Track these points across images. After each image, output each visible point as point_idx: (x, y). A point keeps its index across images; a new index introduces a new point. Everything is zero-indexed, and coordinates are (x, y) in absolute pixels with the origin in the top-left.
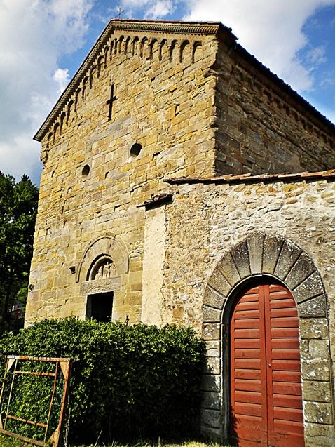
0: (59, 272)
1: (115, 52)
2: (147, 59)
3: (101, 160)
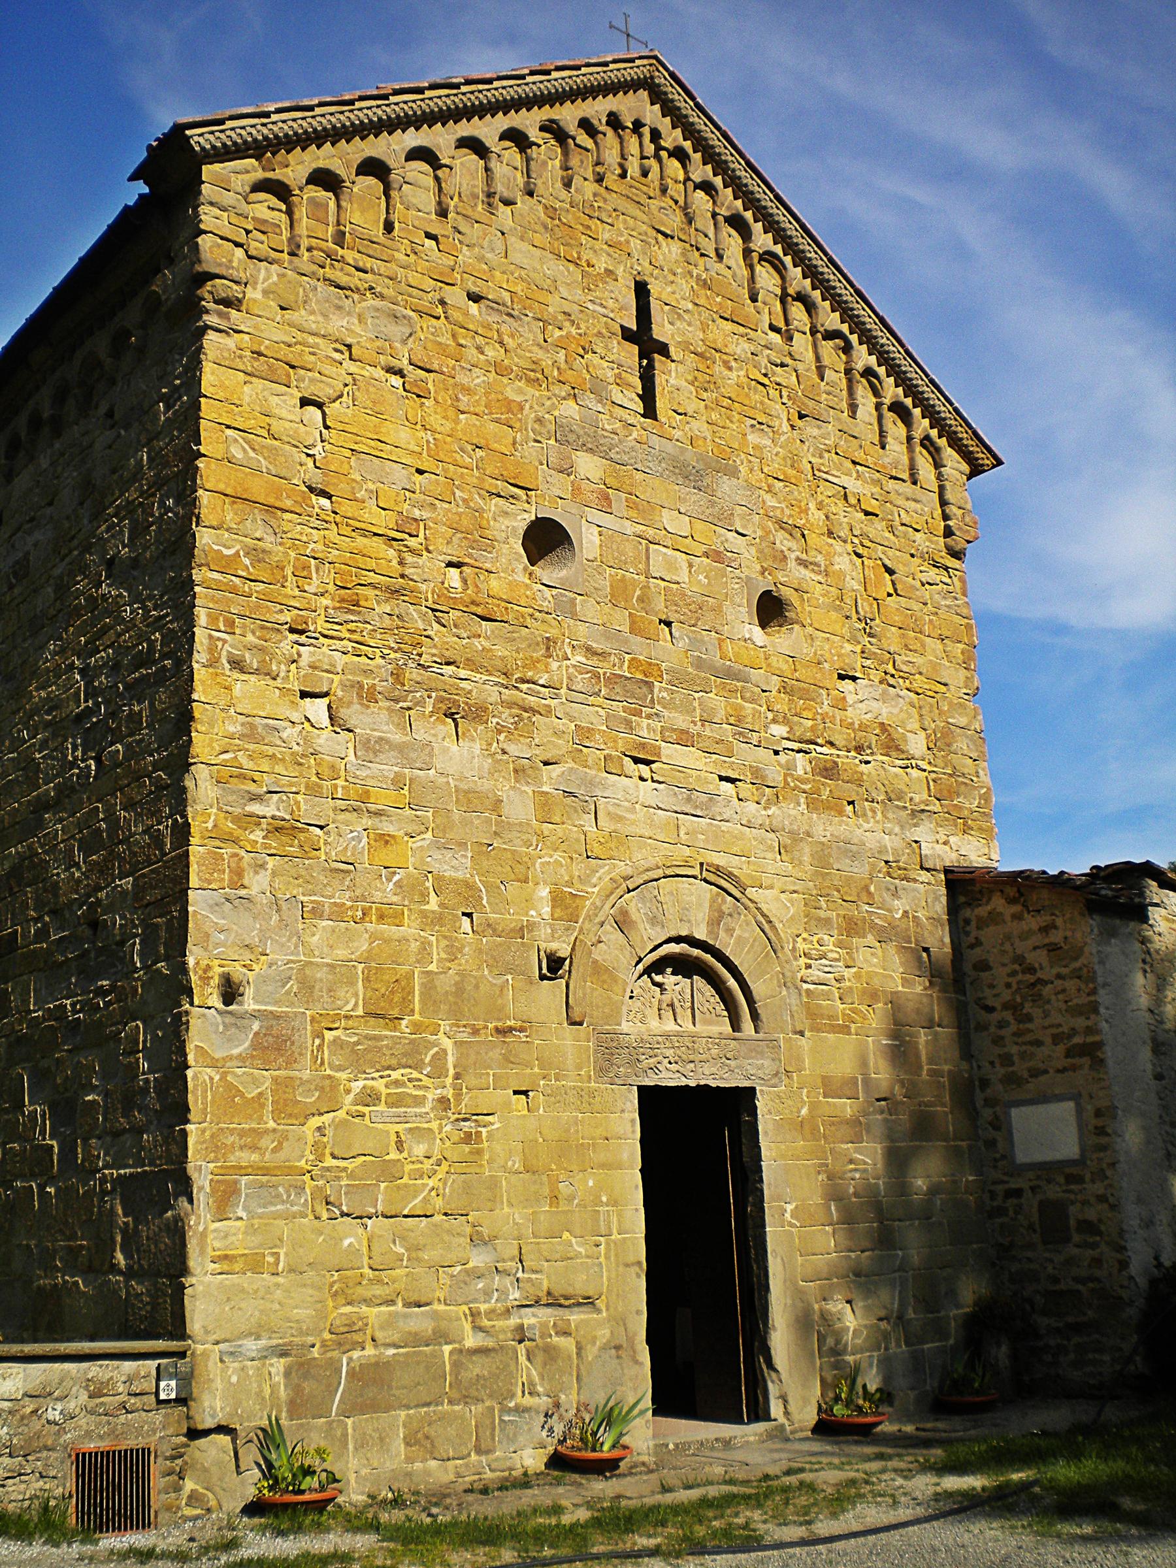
1: (645, 174)
2: (773, 328)
3: (629, 550)
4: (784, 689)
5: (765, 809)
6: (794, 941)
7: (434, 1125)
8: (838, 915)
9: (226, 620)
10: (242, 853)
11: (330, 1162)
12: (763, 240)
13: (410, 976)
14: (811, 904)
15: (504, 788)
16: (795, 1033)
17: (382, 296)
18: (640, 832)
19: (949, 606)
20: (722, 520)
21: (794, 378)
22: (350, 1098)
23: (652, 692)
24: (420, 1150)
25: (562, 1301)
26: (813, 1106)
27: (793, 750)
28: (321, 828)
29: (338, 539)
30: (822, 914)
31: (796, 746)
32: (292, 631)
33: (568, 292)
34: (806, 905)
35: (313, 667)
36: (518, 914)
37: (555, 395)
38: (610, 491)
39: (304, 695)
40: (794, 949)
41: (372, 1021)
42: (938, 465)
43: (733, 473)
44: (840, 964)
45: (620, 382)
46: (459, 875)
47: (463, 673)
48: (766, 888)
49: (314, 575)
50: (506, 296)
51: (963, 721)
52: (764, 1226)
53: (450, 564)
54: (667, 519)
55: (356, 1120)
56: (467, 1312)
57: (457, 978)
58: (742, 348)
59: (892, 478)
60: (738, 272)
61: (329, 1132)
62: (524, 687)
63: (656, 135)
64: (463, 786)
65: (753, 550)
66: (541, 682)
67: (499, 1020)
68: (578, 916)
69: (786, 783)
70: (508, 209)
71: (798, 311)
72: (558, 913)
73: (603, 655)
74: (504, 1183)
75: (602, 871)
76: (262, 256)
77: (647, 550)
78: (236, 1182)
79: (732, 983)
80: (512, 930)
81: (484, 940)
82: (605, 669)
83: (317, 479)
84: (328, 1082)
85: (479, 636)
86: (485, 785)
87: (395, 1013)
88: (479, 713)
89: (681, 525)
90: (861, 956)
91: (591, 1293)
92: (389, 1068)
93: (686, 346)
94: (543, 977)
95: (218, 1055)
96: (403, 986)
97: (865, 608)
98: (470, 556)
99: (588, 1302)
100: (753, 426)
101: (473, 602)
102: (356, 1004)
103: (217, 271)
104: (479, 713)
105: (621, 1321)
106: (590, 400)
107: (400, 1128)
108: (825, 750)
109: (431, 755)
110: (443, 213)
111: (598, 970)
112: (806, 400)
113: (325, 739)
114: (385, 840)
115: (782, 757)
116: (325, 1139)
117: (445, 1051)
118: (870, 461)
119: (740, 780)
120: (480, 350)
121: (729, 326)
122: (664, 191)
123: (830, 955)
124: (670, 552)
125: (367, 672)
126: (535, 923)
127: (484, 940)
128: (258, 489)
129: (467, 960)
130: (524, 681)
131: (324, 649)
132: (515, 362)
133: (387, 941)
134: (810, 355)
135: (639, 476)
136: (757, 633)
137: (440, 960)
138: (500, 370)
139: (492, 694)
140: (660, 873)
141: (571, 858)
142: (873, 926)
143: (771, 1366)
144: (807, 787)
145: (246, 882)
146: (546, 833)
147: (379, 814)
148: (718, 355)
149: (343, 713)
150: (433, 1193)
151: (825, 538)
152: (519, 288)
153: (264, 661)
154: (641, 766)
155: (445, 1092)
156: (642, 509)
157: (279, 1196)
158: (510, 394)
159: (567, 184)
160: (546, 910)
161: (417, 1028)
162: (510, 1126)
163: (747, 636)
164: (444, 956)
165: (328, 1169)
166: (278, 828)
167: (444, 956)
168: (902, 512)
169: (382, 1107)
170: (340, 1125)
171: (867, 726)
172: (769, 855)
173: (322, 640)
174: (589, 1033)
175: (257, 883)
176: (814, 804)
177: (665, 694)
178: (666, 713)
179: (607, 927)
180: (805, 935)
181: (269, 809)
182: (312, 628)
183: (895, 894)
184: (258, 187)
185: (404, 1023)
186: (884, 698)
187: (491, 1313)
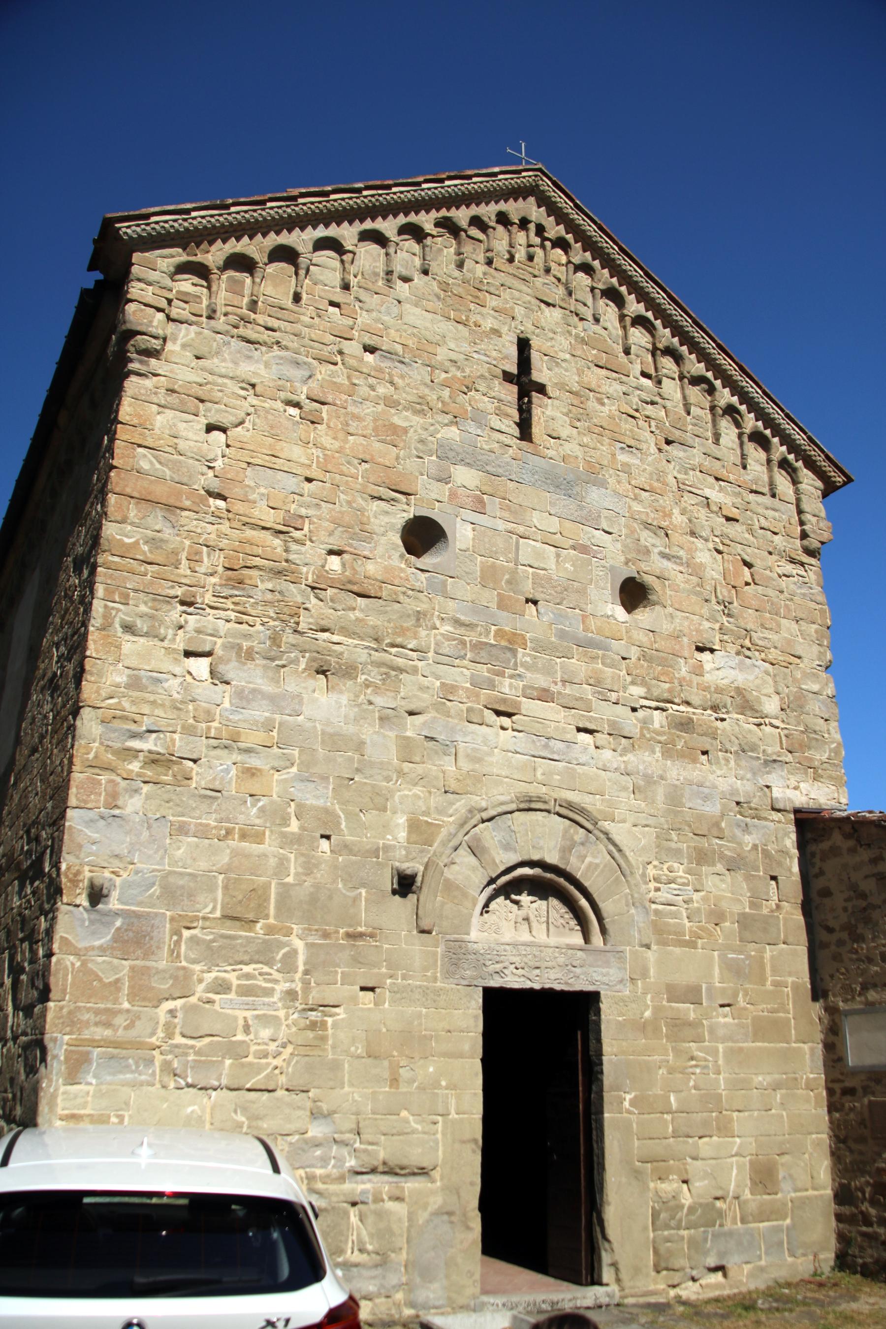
0: (309, 867)
1: (531, 258)
2: (644, 375)
3: (500, 543)
4: (644, 656)
5: (621, 755)
7: (281, 1013)
8: (688, 847)
9: (122, 595)
10: (119, 779)
11: (179, 1040)
12: (634, 307)
13: (266, 887)
14: (662, 837)
15: (369, 732)
16: (642, 946)
17: (286, 348)
18: (499, 772)
19: (804, 595)
20: (590, 520)
21: (663, 413)
22: (200, 988)
23: (515, 656)
24: (265, 1033)
25: (398, 1171)
26: (657, 1010)
27: (650, 708)
28: (195, 761)
29: (229, 531)
30: (673, 845)
31: (654, 704)
32: (183, 603)
33: (453, 342)
34: (657, 837)
35: (198, 631)
36: (375, 837)
37: (438, 422)
38: (485, 496)
39: (188, 654)
40: (644, 875)
41: (229, 923)
42: (795, 482)
43: (603, 484)
44: (690, 888)
45: (499, 413)
46: (320, 803)
47: (336, 638)
48: (619, 822)
49: (205, 559)
50: (399, 349)
51: (815, 687)
52: (602, 1113)
53: (331, 552)
54: (536, 518)
55: (207, 1006)
56: (304, 1175)
57: (312, 890)
58: (615, 388)
59: (752, 491)
60: (614, 332)
61: (180, 1014)
62: (394, 650)
63: (540, 230)
64: (330, 730)
65: (619, 546)
66: (410, 646)
67: (350, 926)
69: (643, 735)
70: (407, 285)
71: (667, 363)
72: (414, 837)
73: (470, 626)
74: (346, 1066)
75: (458, 804)
76: (183, 318)
77: (517, 543)
78: (88, 1053)
79: (584, 902)
80: (367, 851)
81: (340, 859)
82: (471, 637)
83: (216, 485)
84: (181, 973)
85: (354, 609)
86: (351, 729)
87: (251, 916)
88: (349, 671)
89: (553, 524)
90: (710, 882)
91: (424, 1165)
92: (241, 963)
93: (561, 386)
94: (394, 892)
95: (80, 945)
96: (259, 895)
97: (724, 592)
98: (351, 545)
99: (423, 1172)
100: (622, 448)
101: (350, 582)
102: (214, 908)
103: (139, 328)
104: (349, 671)
105: (453, 1190)
106: (472, 427)
107: (249, 1014)
108: (682, 708)
109: (301, 703)
110: (346, 287)
111: (450, 886)
112: (673, 430)
113: (206, 691)
114: (251, 773)
115: (641, 713)
116: (176, 1020)
117: (295, 952)
118: (732, 478)
119: (597, 732)
120: (372, 388)
121: (604, 372)
122: (548, 271)
123: (679, 880)
124: (538, 545)
125: (247, 636)
127: (340, 859)
128: (160, 492)
129: (321, 875)
130: (393, 645)
131: (210, 618)
132: (402, 397)
133: (248, 856)
134: (679, 395)
135: (511, 485)
136: (620, 612)
137: (297, 874)
138: (390, 403)
139: (362, 656)
140: (513, 806)
141: (430, 792)
142: (722, 857)
143: (605, 1238)
144: (663, 738)
145: (120, 803)
146: (406, 770)
147: (248, 751)
148: (591, 394)
149: (221, 668)
150: (277, 1071)
151: (688, 537)
152: (410, 343)
153: (153, 626)
154: (502, 718)
155: (293, 986)
156: (516, 512)
157: (128, 1066)
158: (397, 420)
159: (460, 265)
160: (402, 835)
161: (270, 930)
162: (353, 1018)
163: (610, 613)
164: (300, 870)
165: (177, 1046)
166: (154, 760)
167: (300, 870)
168: (762, 519)
169: (232, 996)
170: (190, 1010)
171: (722, 690)
172: (624, 794)
173: (208, 610)
174: (438, 940)
175: (133, 805)
176: (668, 752)
177: (528, 659)
178: (529, 675)
179: (461, 851)
180: (655, 863)
181: (149, 744)
182: (199, 601)
183: (746, 828)
184: (183, 269)
185: (259, 925)
186: (741, 667)
187: (326, 1179)
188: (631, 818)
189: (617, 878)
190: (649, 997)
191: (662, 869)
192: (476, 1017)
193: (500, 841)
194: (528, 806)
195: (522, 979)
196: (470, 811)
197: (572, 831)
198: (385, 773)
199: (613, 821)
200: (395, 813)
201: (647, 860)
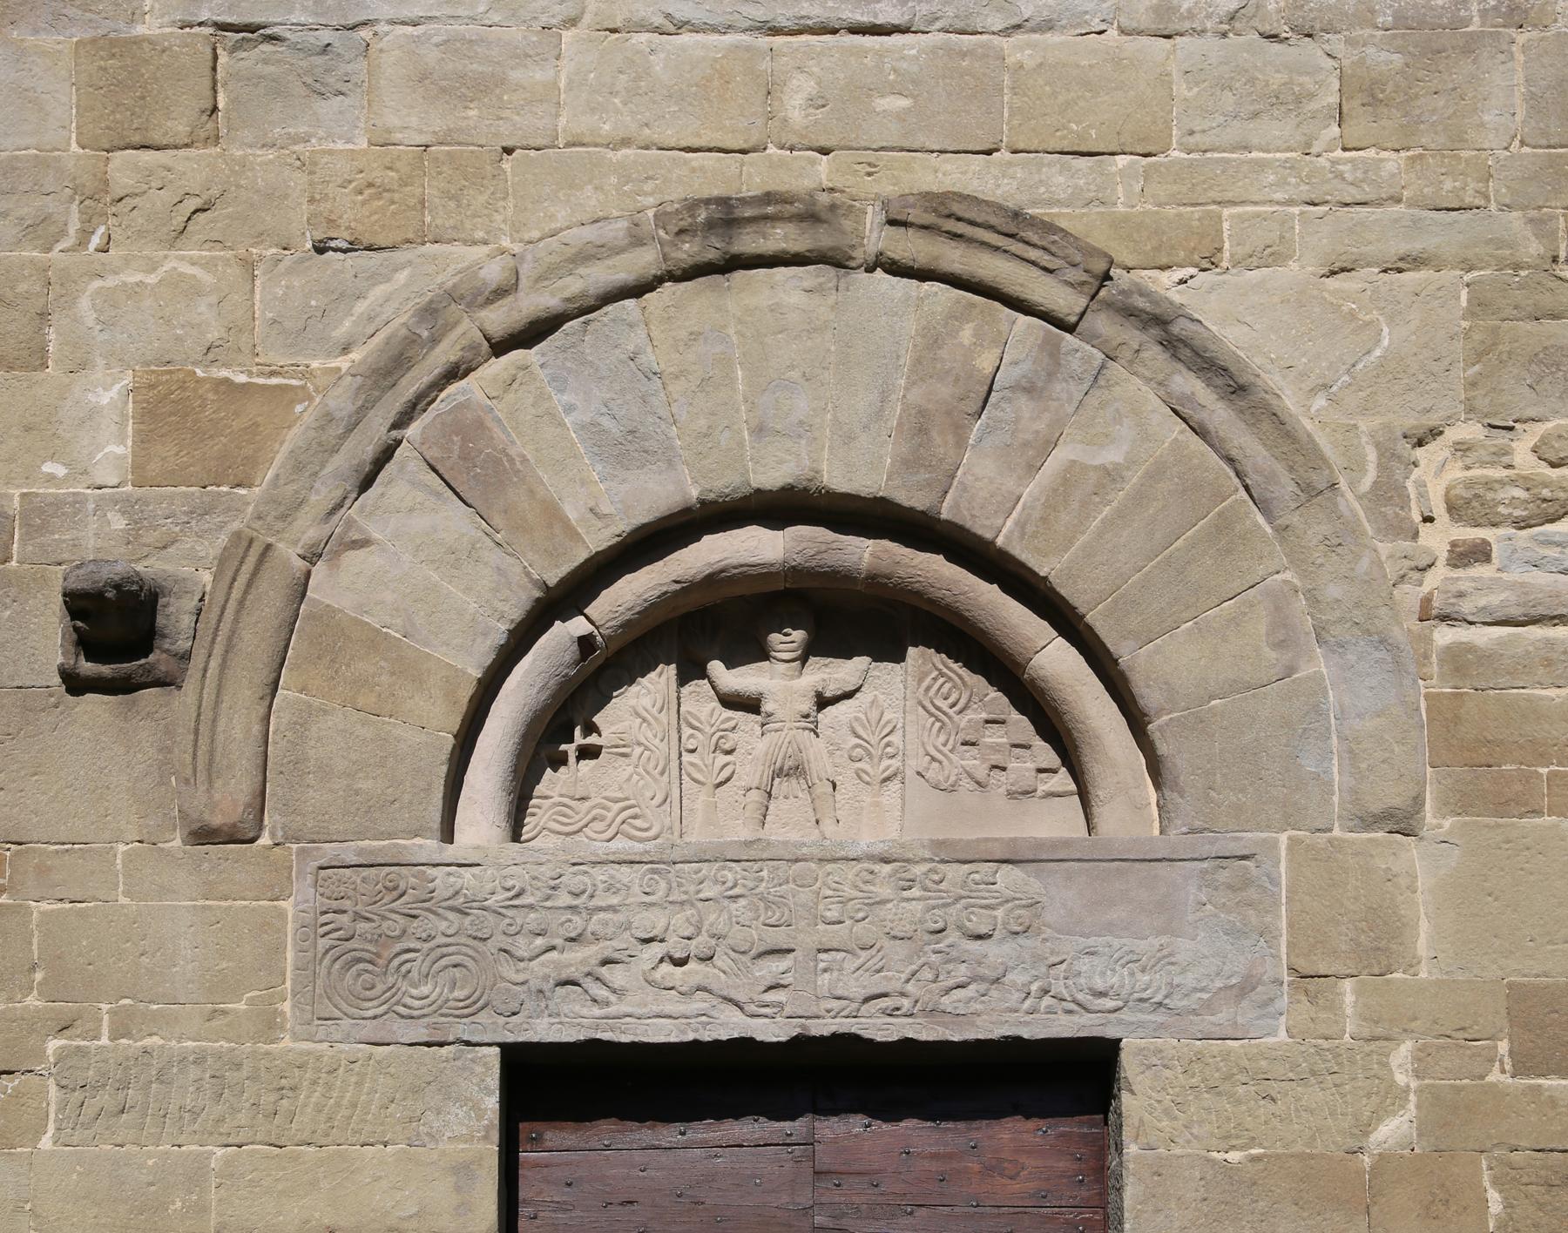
6: (1388, 456)
16: (1369, 821)
34: (1479, 305)
40: (1388, 493)
48: (1245, 262)
68: (253, 462)
75: (379, 291)
94: (75, 684)
126: (57, 504)
140: (645, 261)
160: (111, 453)
172: (1277, 129)
180: (1471, 431)
188: (1318, 238)
189: (1224, 524)
190: (1402, 1053)
191: (1501, 456)
192: (463, 1171)
193: (591, 429)
194: (721, 245)
195: (699, 1003)
196: (429, 312)
197: (966, 335)
198: (29, 209)
199: (1210, 262)
200: (81, 366)
201: (1412, 421)
